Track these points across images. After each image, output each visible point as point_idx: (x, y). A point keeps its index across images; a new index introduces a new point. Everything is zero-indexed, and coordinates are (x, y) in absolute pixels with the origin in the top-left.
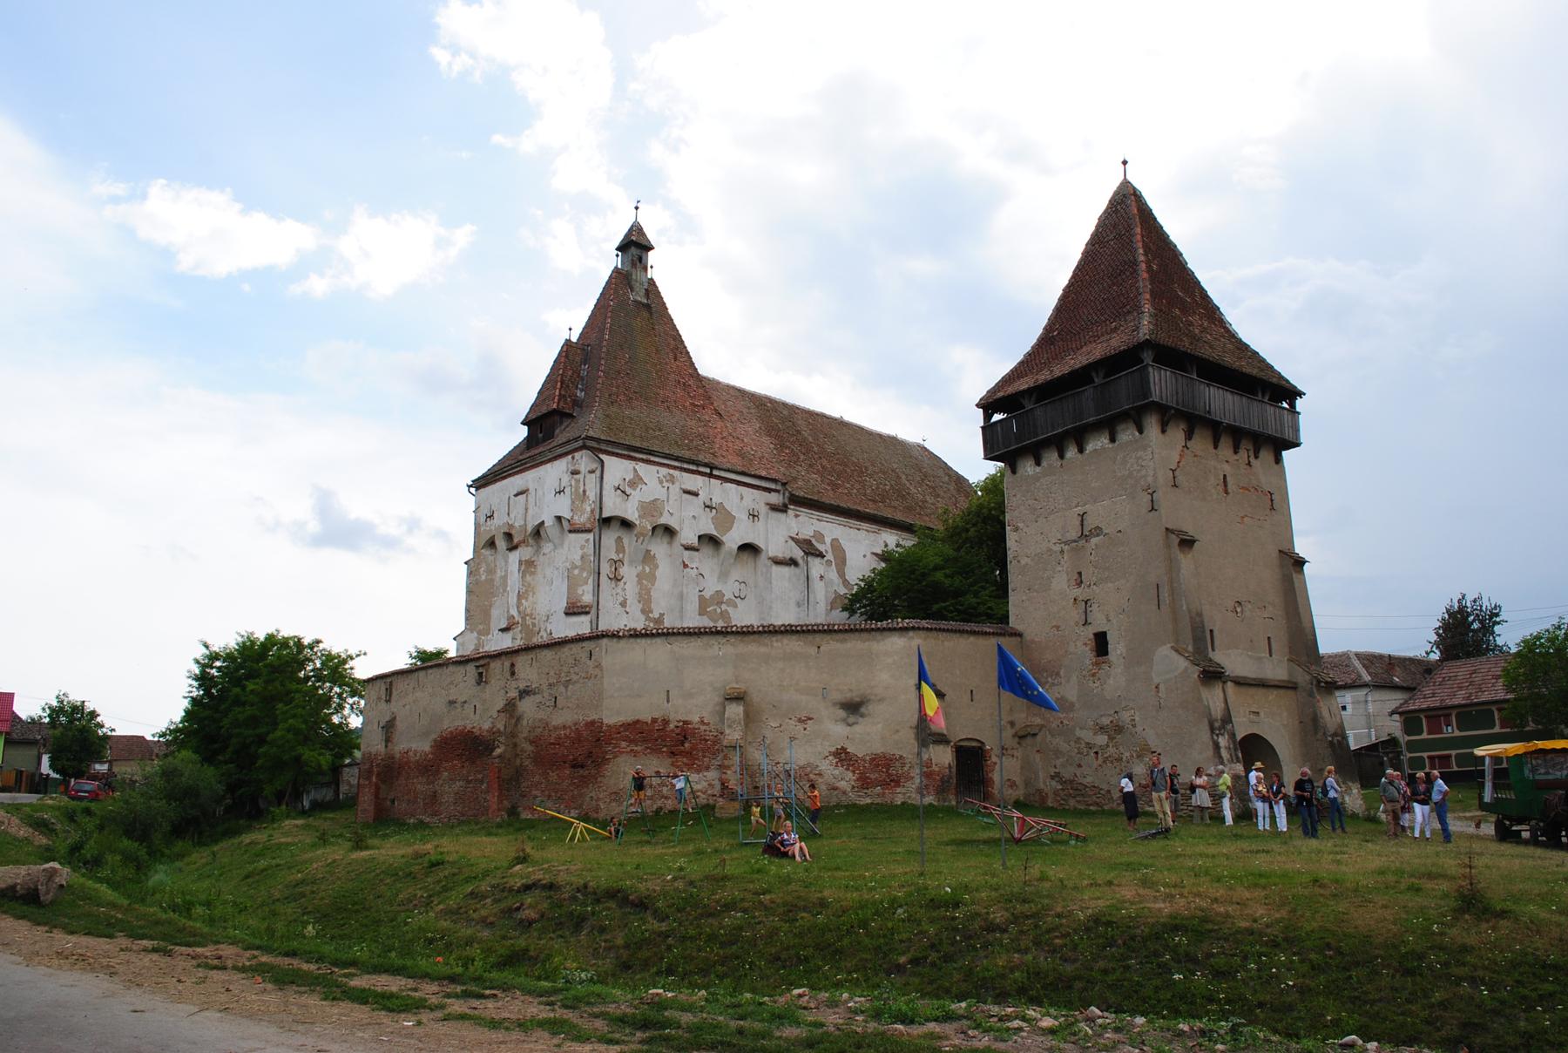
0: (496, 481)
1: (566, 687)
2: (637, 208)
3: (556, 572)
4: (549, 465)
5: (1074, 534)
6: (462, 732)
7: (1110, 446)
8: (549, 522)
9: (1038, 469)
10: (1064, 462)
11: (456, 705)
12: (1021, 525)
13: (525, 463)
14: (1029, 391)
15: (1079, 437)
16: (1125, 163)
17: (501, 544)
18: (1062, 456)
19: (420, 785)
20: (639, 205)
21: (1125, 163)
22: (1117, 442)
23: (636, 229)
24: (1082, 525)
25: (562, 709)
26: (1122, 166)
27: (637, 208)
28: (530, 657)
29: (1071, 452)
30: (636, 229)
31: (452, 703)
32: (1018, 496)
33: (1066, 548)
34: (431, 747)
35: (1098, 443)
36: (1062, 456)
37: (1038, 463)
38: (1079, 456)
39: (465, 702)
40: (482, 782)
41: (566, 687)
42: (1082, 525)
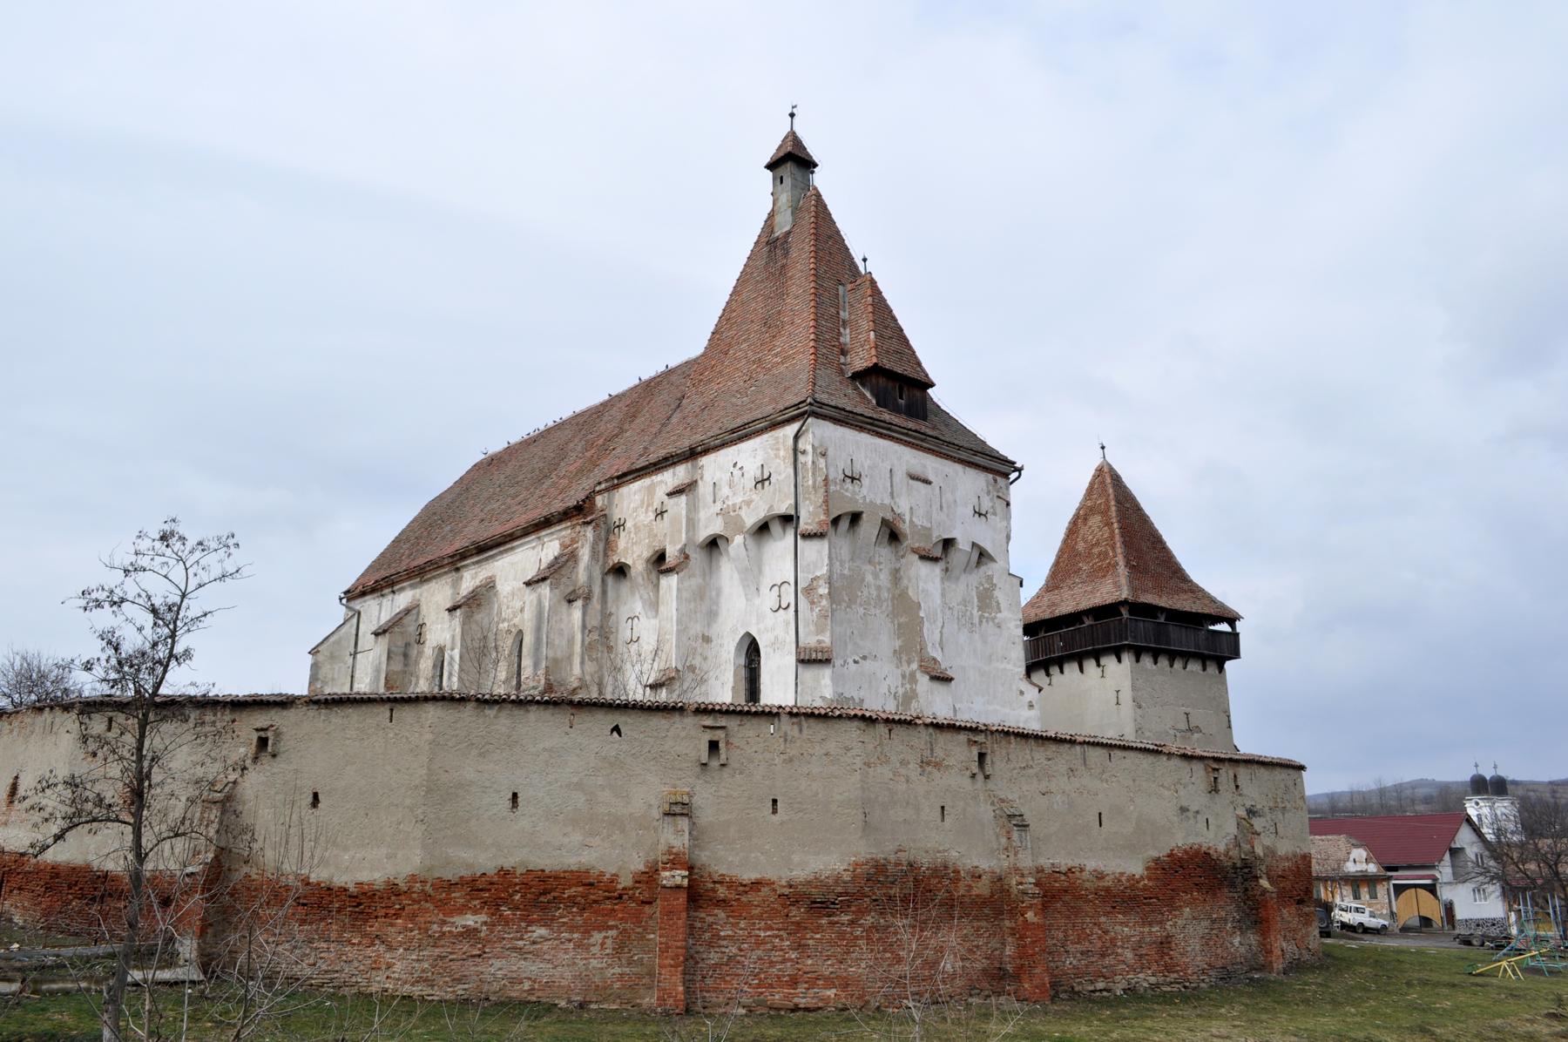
0: (861, 429)
1: (1284, 814)
2: (792, 115)
3: (948, 612)
4: (958, 467)
5: (1183, 726)
6: (1197, 853)
7: (1202, 672)
8: (963, 545)
9: (1154, 667)
10: (1173, 670)
11: (1187, 813)
12: (1143, 704)
13: (922, 440)
14: (1163, 609)
15: (1187, 656)
16: (1103, 448)
17: (869, 528)
18: (1172, 666)
19: (1125, 929)
20: (795, 111)
21: (1103, 448)
22: (1206, 672)
23: (793, 138)
24: (1188, 721)
25: (1282, 838)
26: (1102, 451)
27: (792, 115)
28: (1250, 771)
29: (1178, 665)
30: (793, 138)
31: (1184, 810)
32: (1140, 681)
33: (1178, 734)
34: (1148, 869)
35: (1194, 666)
36: (1172, 666)
37: (1156, 663)
38: (1183, 671)
39: (1197, 812)
40: (1225, 920)
41: (1284, 814)
42: (1188, 721)
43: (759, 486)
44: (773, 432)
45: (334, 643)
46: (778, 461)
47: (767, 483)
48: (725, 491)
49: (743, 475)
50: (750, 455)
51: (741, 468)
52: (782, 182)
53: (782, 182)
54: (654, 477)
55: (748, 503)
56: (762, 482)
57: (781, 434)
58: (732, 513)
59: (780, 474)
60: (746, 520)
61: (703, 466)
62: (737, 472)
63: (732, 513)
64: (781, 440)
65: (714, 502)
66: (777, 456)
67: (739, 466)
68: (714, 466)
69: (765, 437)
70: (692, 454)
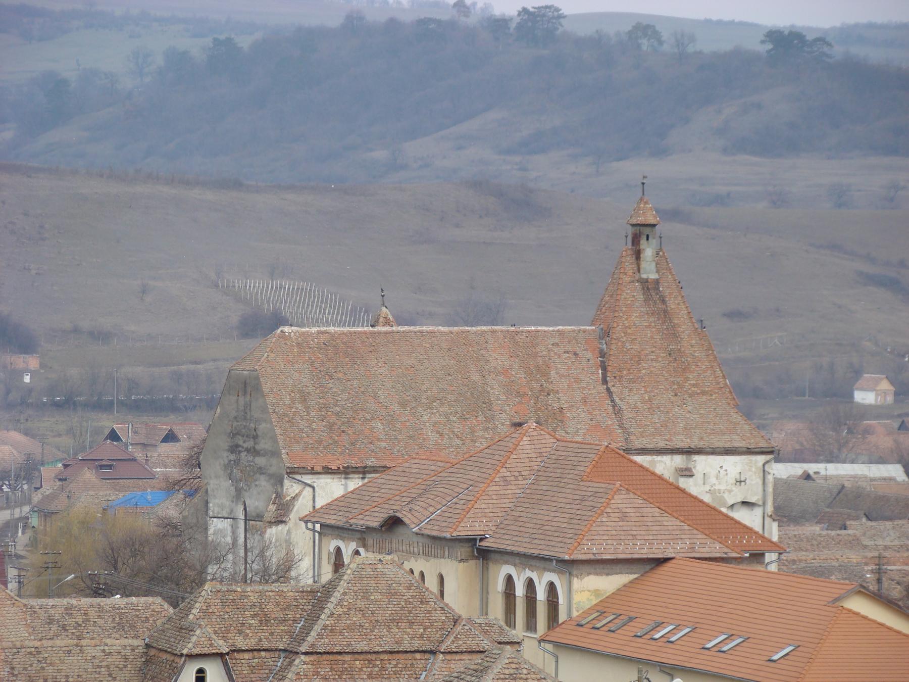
43: (738, 483)
44: (749, 456)
45: (296, 511)
46: (751, 473)
47: (743, 483)
48: (713, 480)
49: (727, 474)
50: (733, 465)
51: (726, 470)
52: (648, 239)
53: (648, 239)
54: (655, 457)
55: (730, 491)
56: (740, 482)
57: (754, 459)
58: (717, 494)
59: (752, 480)
60: (728, 500)
61: (695, 461)
62: (722, 471)
63: (717, 494)
64: (753, 462)
65: (704, 484)
66: (750, 470)
67: (724, 468)
68: (702, 463)
69: (743, 457)
70: (689, 452)
